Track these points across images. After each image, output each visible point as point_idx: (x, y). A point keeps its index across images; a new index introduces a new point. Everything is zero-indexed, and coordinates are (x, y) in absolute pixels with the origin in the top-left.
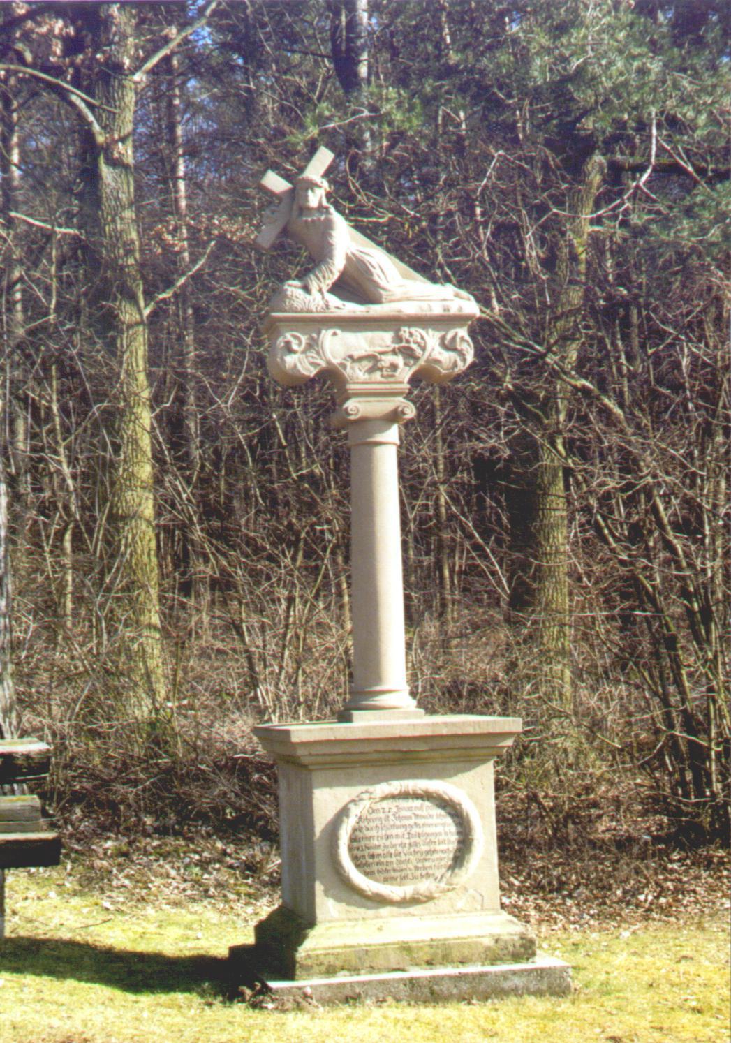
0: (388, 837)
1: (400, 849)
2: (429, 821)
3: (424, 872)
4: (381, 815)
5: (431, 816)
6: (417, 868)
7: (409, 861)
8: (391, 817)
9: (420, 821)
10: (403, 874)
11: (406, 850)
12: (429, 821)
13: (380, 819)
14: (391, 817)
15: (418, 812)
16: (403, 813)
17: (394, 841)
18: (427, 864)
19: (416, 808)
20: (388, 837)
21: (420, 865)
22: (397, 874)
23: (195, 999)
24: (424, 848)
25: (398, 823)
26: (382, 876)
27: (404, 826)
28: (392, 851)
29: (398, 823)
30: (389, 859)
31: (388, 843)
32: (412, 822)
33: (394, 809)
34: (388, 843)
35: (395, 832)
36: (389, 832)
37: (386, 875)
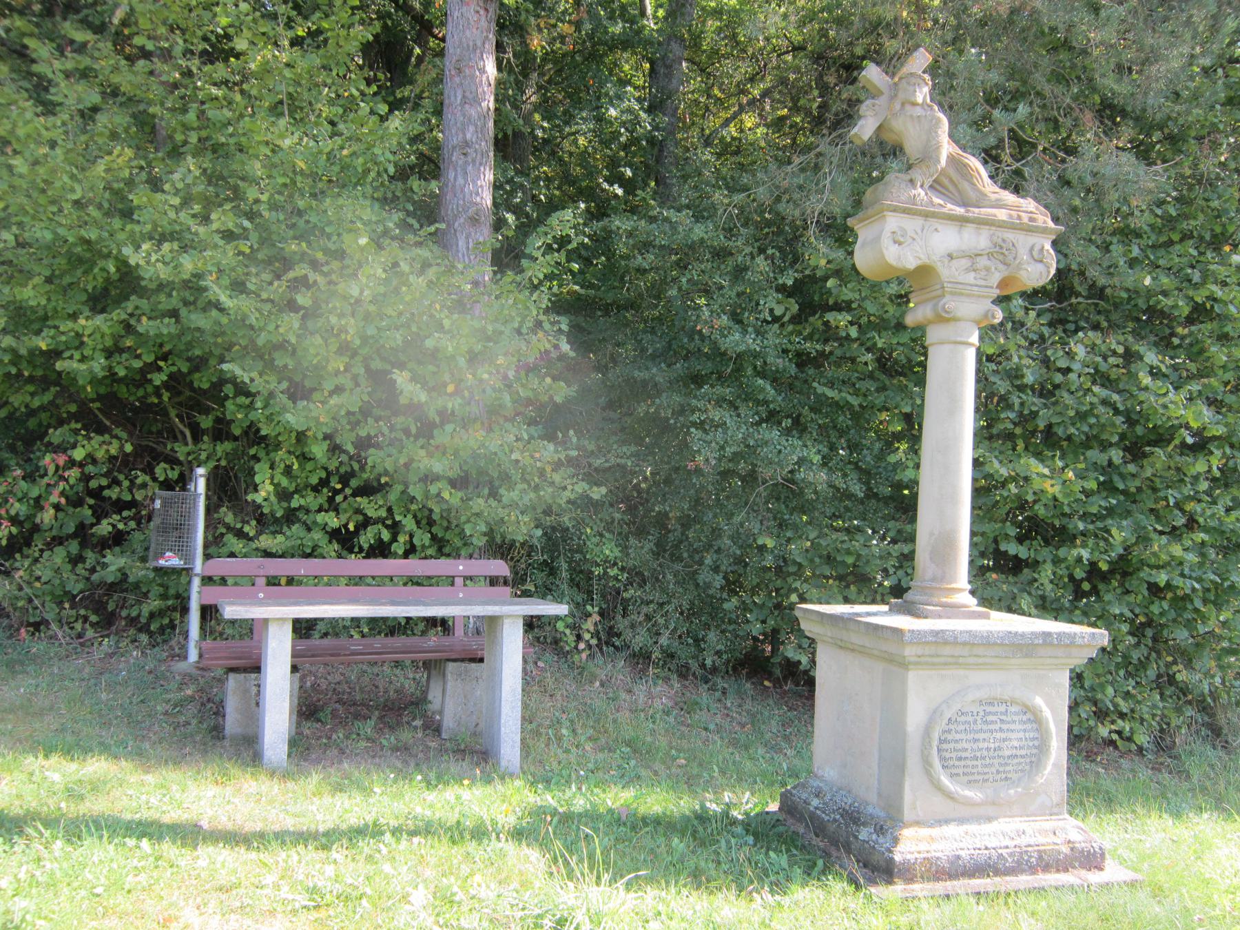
0: (976, 741)
1: (985, 753)
2: (1012, 727)
3: (1004, 776)
4: (970, 719)
5: (1014, 722)
6: (998, 772)
7: (991, 765)
8: (979, 721)
9: (1005, 727)
10: (986, 777)
11: (991, 753)
12: (1012, 727)
13: (969, 723)
14: (979, 721)
15: (1004, 717)
16: (990, 718)
17: (981, 745)
18: (1008, 768)
19: (1002, 713)
20: (976, 741)
21: (1001, 769)
22: (980, 777)
23: (838, 886)
24: (1007, 753)
25: (985, 727)
26: (966, 778)
27: (991, 731)
28: (978, 754)
29: (985, 727)
30: (975, 763)
31: (975, 746)
32: (997, 727)
33: (982, 713)
34: (975, 746)
35: (981, 736)
36: (977, 736)
37: (971, 778)
